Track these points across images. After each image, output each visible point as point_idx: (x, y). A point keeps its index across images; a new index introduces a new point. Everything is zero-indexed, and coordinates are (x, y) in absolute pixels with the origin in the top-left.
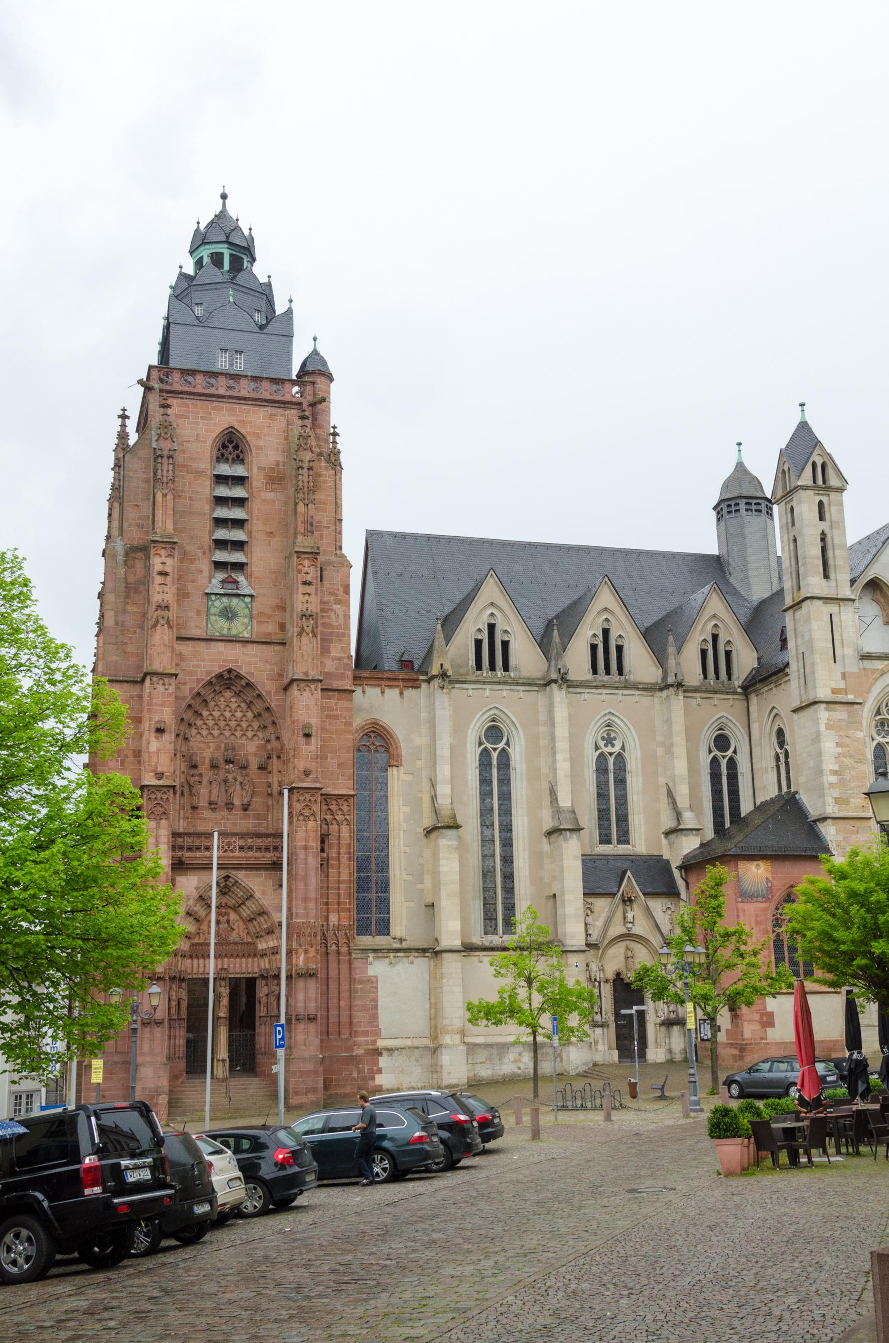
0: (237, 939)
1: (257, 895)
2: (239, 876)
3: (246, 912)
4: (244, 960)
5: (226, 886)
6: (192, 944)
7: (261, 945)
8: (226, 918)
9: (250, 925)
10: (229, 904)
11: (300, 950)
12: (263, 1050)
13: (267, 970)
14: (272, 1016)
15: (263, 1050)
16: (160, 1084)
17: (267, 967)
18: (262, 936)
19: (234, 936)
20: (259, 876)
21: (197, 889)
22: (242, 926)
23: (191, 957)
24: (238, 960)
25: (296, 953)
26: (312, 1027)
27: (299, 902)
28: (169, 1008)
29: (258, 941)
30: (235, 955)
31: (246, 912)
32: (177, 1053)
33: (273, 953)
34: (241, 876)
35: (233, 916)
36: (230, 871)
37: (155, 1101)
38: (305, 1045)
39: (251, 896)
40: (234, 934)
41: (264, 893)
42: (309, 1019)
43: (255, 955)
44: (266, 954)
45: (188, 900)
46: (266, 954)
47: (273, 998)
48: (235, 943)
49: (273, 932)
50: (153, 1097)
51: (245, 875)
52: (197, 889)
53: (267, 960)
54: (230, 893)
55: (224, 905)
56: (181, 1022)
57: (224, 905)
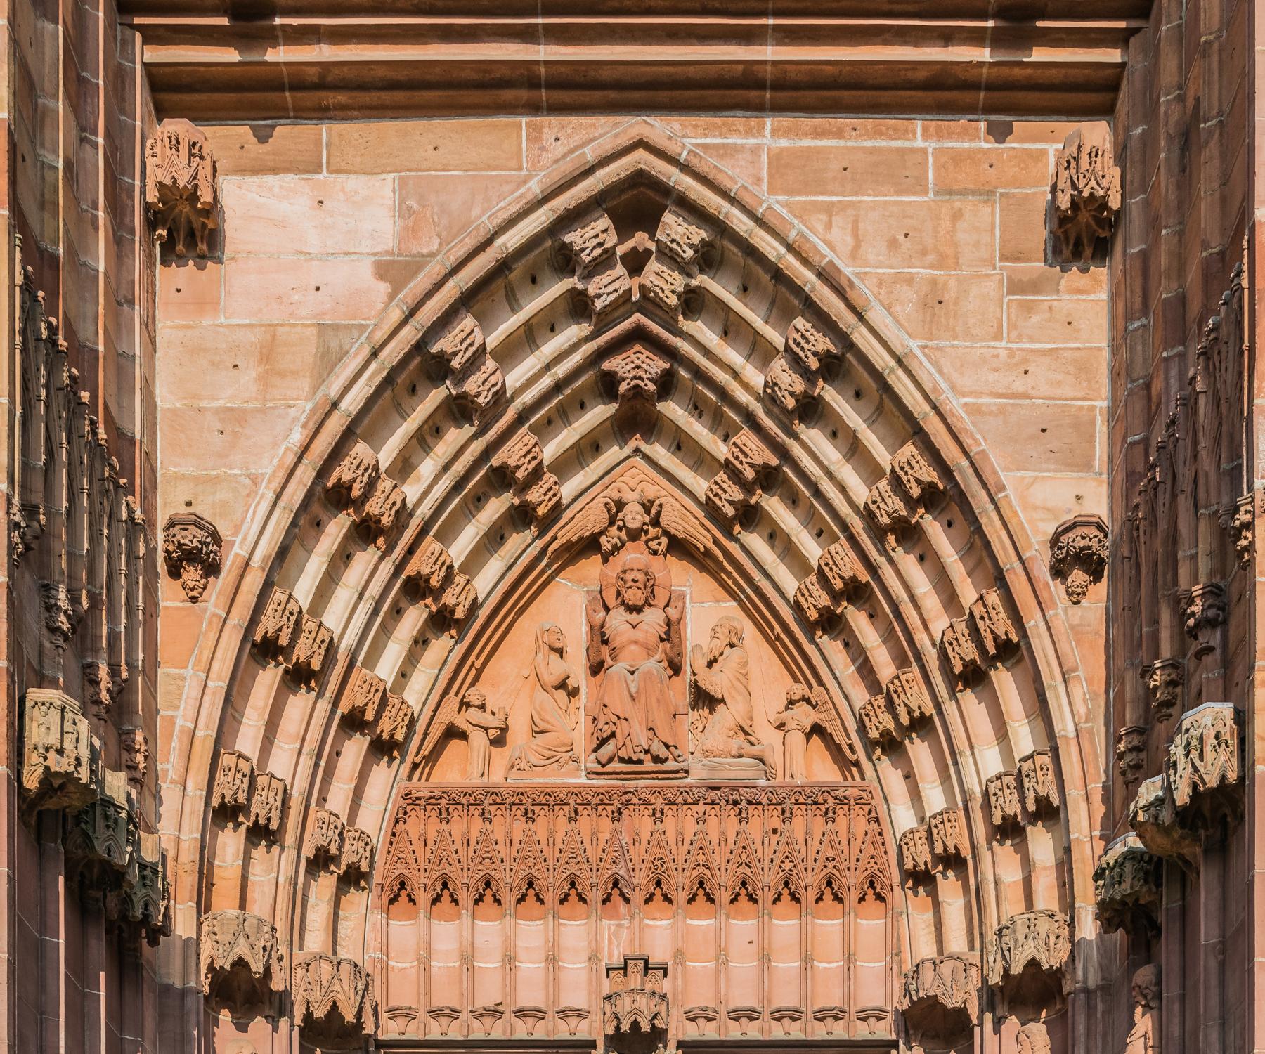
2: (734, 174)
21: (392, 271)
36: (659, 128)
52: (392, 271)
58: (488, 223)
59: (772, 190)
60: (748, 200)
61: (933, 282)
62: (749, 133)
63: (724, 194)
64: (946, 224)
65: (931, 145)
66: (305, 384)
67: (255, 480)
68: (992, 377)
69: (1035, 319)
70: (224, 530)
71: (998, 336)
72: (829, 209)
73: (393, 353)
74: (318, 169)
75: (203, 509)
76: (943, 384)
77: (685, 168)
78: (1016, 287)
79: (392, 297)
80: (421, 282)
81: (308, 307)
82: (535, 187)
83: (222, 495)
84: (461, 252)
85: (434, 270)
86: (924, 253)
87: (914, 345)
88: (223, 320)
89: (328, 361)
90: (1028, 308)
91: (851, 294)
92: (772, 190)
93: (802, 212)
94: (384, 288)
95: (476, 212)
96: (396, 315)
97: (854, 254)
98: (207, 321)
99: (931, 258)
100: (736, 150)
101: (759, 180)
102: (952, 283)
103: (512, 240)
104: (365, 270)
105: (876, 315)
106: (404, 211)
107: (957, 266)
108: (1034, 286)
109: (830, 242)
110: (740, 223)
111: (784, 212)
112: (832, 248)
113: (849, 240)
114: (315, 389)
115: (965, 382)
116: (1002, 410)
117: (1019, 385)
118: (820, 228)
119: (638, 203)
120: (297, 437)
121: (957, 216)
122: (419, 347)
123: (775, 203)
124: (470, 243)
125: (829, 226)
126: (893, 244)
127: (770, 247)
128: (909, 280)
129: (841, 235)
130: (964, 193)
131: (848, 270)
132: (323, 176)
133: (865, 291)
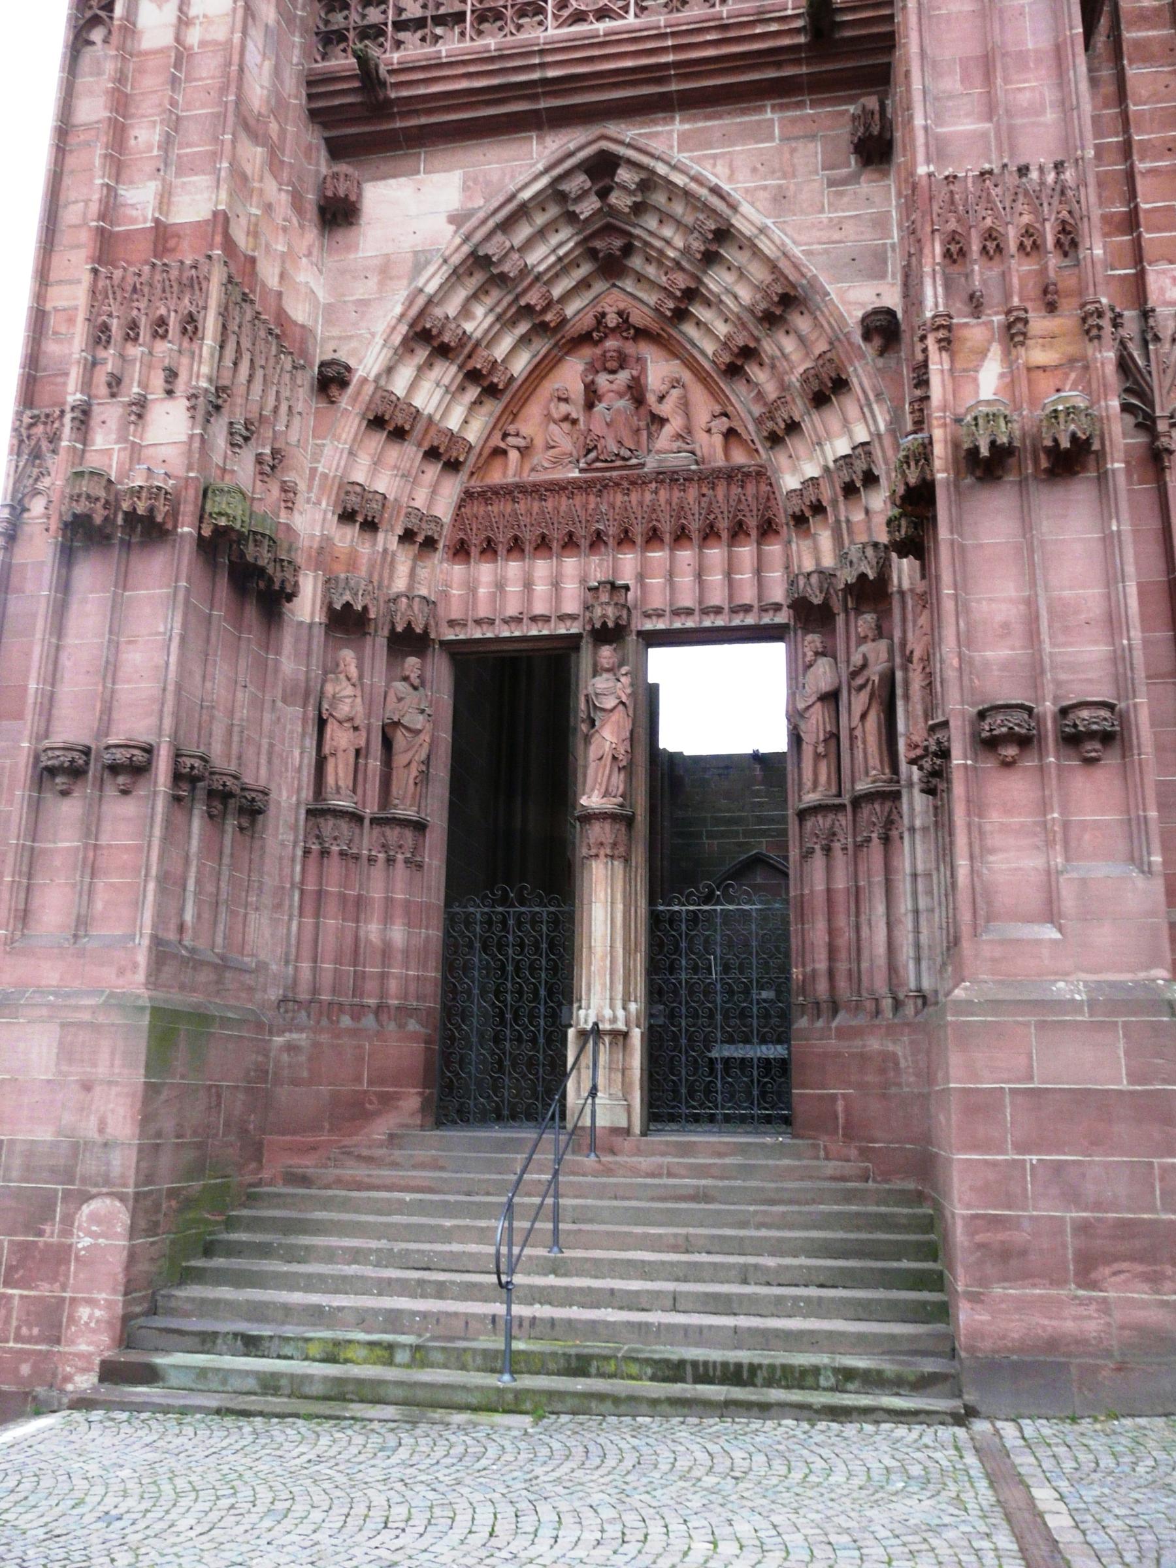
0: (679, 460)
1: (749, 217)
2: (656, 146)
3: (710, 332)
4: (716, 554)
5: (610, 224)
6: (468, 496)
7: (796, 470)
8: (623, 377)
9: (740, 396)
10: (639, 317)
11: (974, 332)
12: (822, 986)
13: (827, 576)
14: (858, 801)
15: (822, 987)
16: (89, 1129)
17: (828, 561)
18: (793, 427)
19: (664, 451)
20: (761, 133)
21: (456, 219)
22: (703, 408)
23: (461, 551)
24: (686, 555)
25: (946, 344)
26: (1093, 797)
27: (951, 83)
28: (321, 763)
29: (781, 458)
30: (667, 528)
31: (710, 332)
32: (371, 985)
33: (850, 490)
34: (675, 147)
35: (658, 370)
36: (613, 129)
37: (51, 1235)
38: (1051, 914)
39: (724, 234)
40: (664, 438)
41: (780, 198)
42: (1072, 740)
43: (768, 529)
44: (818, 509)
45: (418, 268)
46: (818, 509)
47: (860, 701)
48: (670, 478)
49: (840, 385)
50: (43, 1208)
51: (684, 138)
52: (456, 219)
53: (825, 539)
54: (636, 262)
55: (612, 320)
56: (393, 834)
57: (612, 320)
58: (512, 188)
59: (679, 151)
60: (665, 157)
61: (780, 186)
62: (666, 124)
63: (652, 156)
64: (787, 155)
65: (776, 116)
66: (405, 282)
67: (373, 335)
68: (818, 234)
69: (845, 199)
70: (352, 363)
71: (822, 211)
72: (714, 157)
73: (456, 259)
74: (418, 172)
75: (342, 356)
76: (788, 241)
77: (629, 146)
78: (832, 183)
79: (456, 232)
80: (473, 222)
81: (408, 243)
82: (540, 167)
83: (354, 344)
84: (496, 204)
85: (481, 215)
86: (773, 172)
87: (769, 222)
88: (360, 254)
89: (418, 268)
90: (840, 194)
91: (730, 200)
92: (679, 151)
93: (698, 160)
94: (452, 228)
95: (507, 180)
96: (458, 240)
97: (731, 179)
98: (352, 256)
99: (778, 174)
100: (657, 134)
101: (671, 147)
102: (792, 187)
103: (526, 195)
104: (443, 219)
105: (745, 208)
106: (465, 188)
107: (794, 176)
108: (844, 182)
109: (716, 174)
110: (661, 169)
111: (687, 162)
112: (716, 175)
113: (727, 171)
114: (410, 284)
115: (803, 238)
116: (826, 251)
117: (837, 236)
118: (709, 167)
119: (602, 167)
120: (398, 310)
121: (793, 151)
122: (473, 253)
123: (683, 158)
124: (501, 199)
125: (714, 165)
126: (754, 170)
127: (679, 179)
128: (765, 188)
129: (722, 169)
130: (797, 138)
131: (726, 187)
132: (422, 176)
133: (737, 196)
